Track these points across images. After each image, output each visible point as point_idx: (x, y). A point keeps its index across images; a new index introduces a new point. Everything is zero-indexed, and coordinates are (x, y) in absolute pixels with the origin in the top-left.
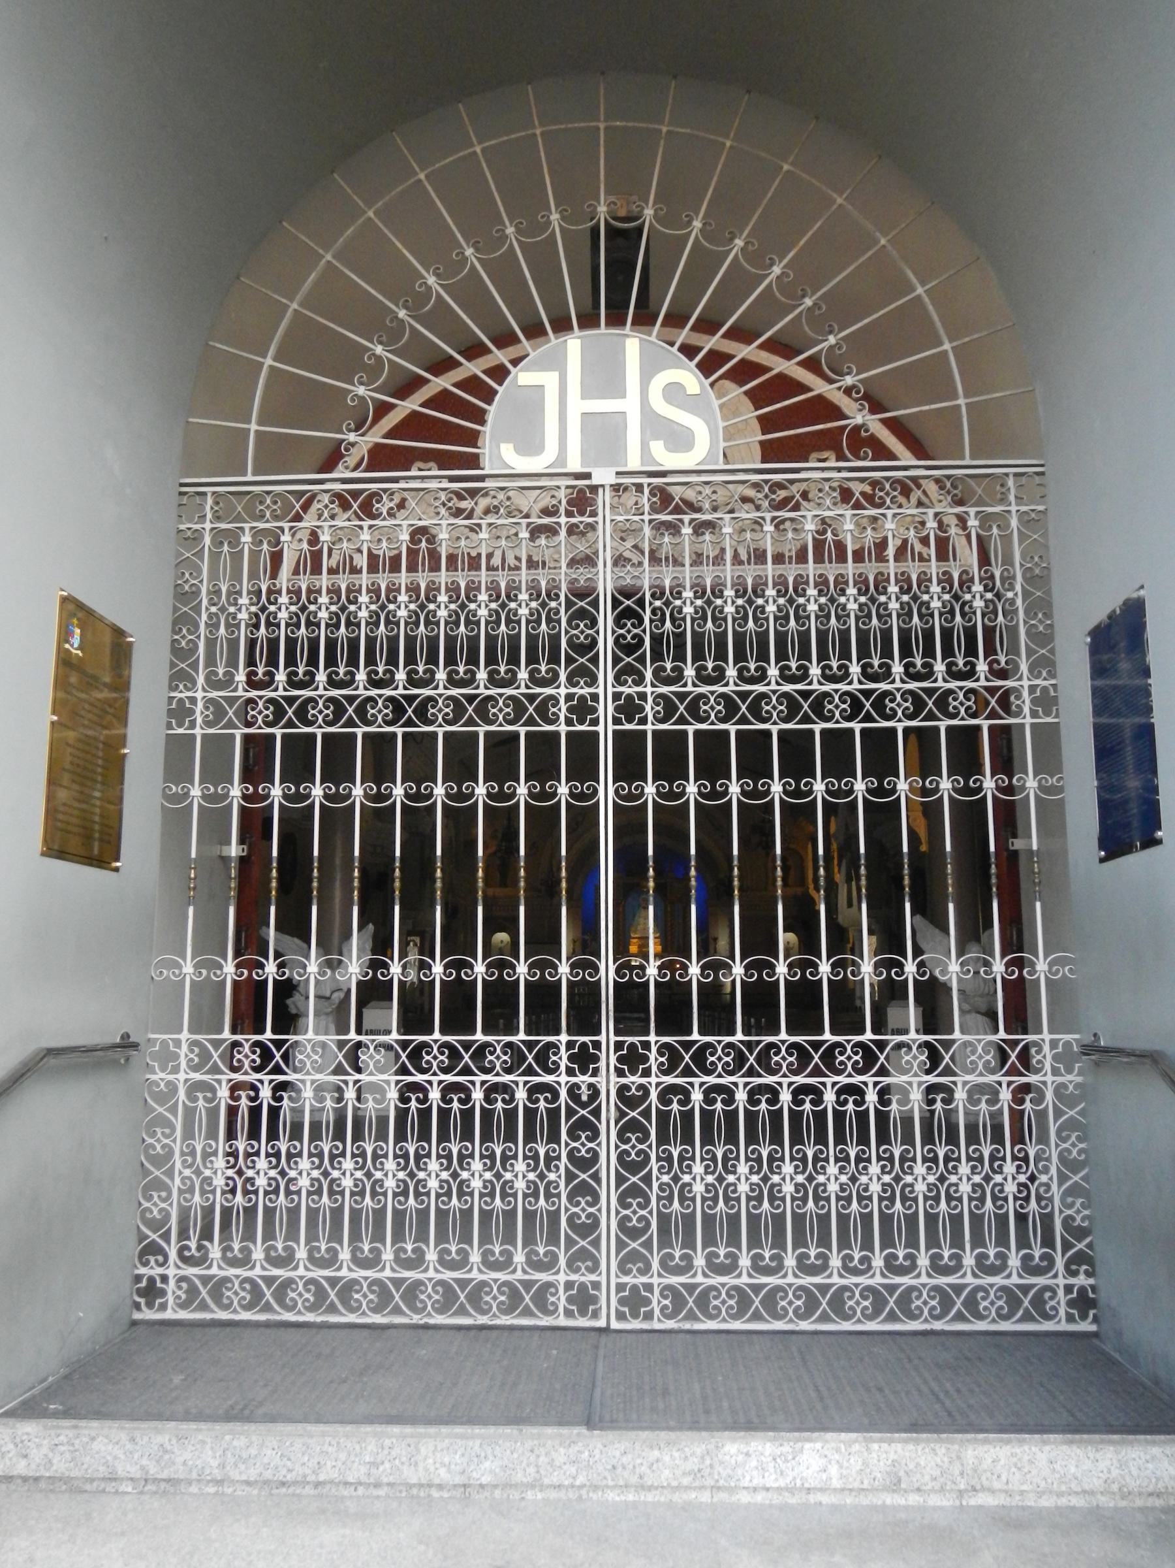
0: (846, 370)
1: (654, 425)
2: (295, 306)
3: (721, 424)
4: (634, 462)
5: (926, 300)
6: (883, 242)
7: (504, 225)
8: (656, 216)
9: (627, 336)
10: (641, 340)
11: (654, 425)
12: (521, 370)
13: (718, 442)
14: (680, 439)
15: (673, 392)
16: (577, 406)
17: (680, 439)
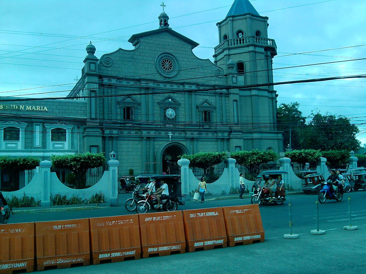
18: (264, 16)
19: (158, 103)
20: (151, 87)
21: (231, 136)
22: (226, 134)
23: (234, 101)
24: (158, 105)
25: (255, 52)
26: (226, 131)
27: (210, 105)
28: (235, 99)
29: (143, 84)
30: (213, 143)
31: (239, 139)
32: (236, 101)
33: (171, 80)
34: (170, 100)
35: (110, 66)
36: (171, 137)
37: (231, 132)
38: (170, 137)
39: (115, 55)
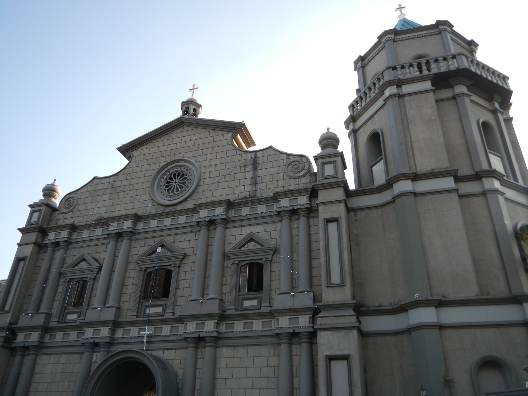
18: (434, 22)
19: (138, 262)
20: (124, 231)
21: (320, 322)
22: (304, 321)
23: (329, 221)
24: (138, 267)
25: (400, 96)
26: (302, 311)
27: (262, 245)
28: (329, 216)
29: (113, 227)
30: (265, 351)
31: (342, 333)
32: (334, 220)
33: (179, 208)
34: (159, 250)
35: (71, 211)
36: (145, 341)
37: (316, 312)
38: (145, 340)
39: (85, 189)
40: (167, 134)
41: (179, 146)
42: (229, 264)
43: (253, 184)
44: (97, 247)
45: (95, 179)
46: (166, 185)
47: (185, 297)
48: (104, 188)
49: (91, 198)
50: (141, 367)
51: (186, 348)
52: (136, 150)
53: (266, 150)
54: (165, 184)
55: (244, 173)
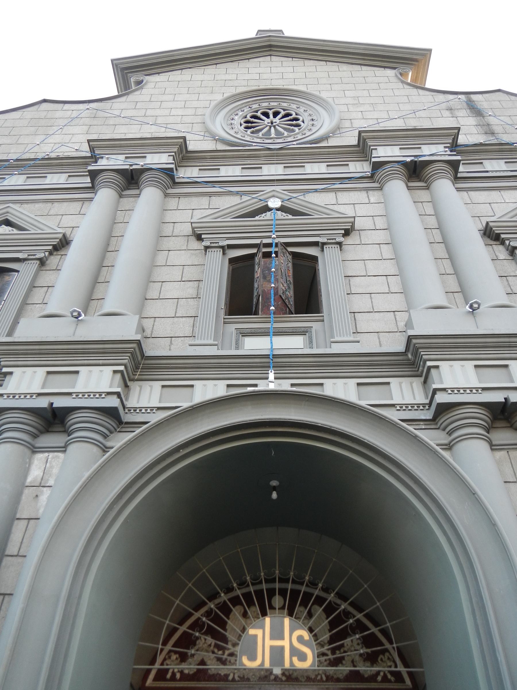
0: (356, 632)
1: (294, 651)
2: (178, 602)
3: (316, 652)
4: (287, 665)
5: (380, 607)
6: (366, 586)
7: (246, 576)
8: (294, 575)
9: (285, 617)
10: (289, 619)
11: (294, 651)
12: (250, 628)
13: (315, 658)
14: (303, 657)
15: (300, 639)
16: (269, 643)
17: (303, 657)
24: (195, 244)
40: (232, 62)
41: (265, 76)
42: (498, 254)
43: (486, 133)
44: (49, 205)
45: (44, 105)
46: (245, 125)
47: (382, 314)
48: (72, 117)
49: (33, 129)
50: (274, 495)
51: (446, 445)
52: (157, 75)
53: (492, 94)
54: (242, 122)
55: (455, 119)
